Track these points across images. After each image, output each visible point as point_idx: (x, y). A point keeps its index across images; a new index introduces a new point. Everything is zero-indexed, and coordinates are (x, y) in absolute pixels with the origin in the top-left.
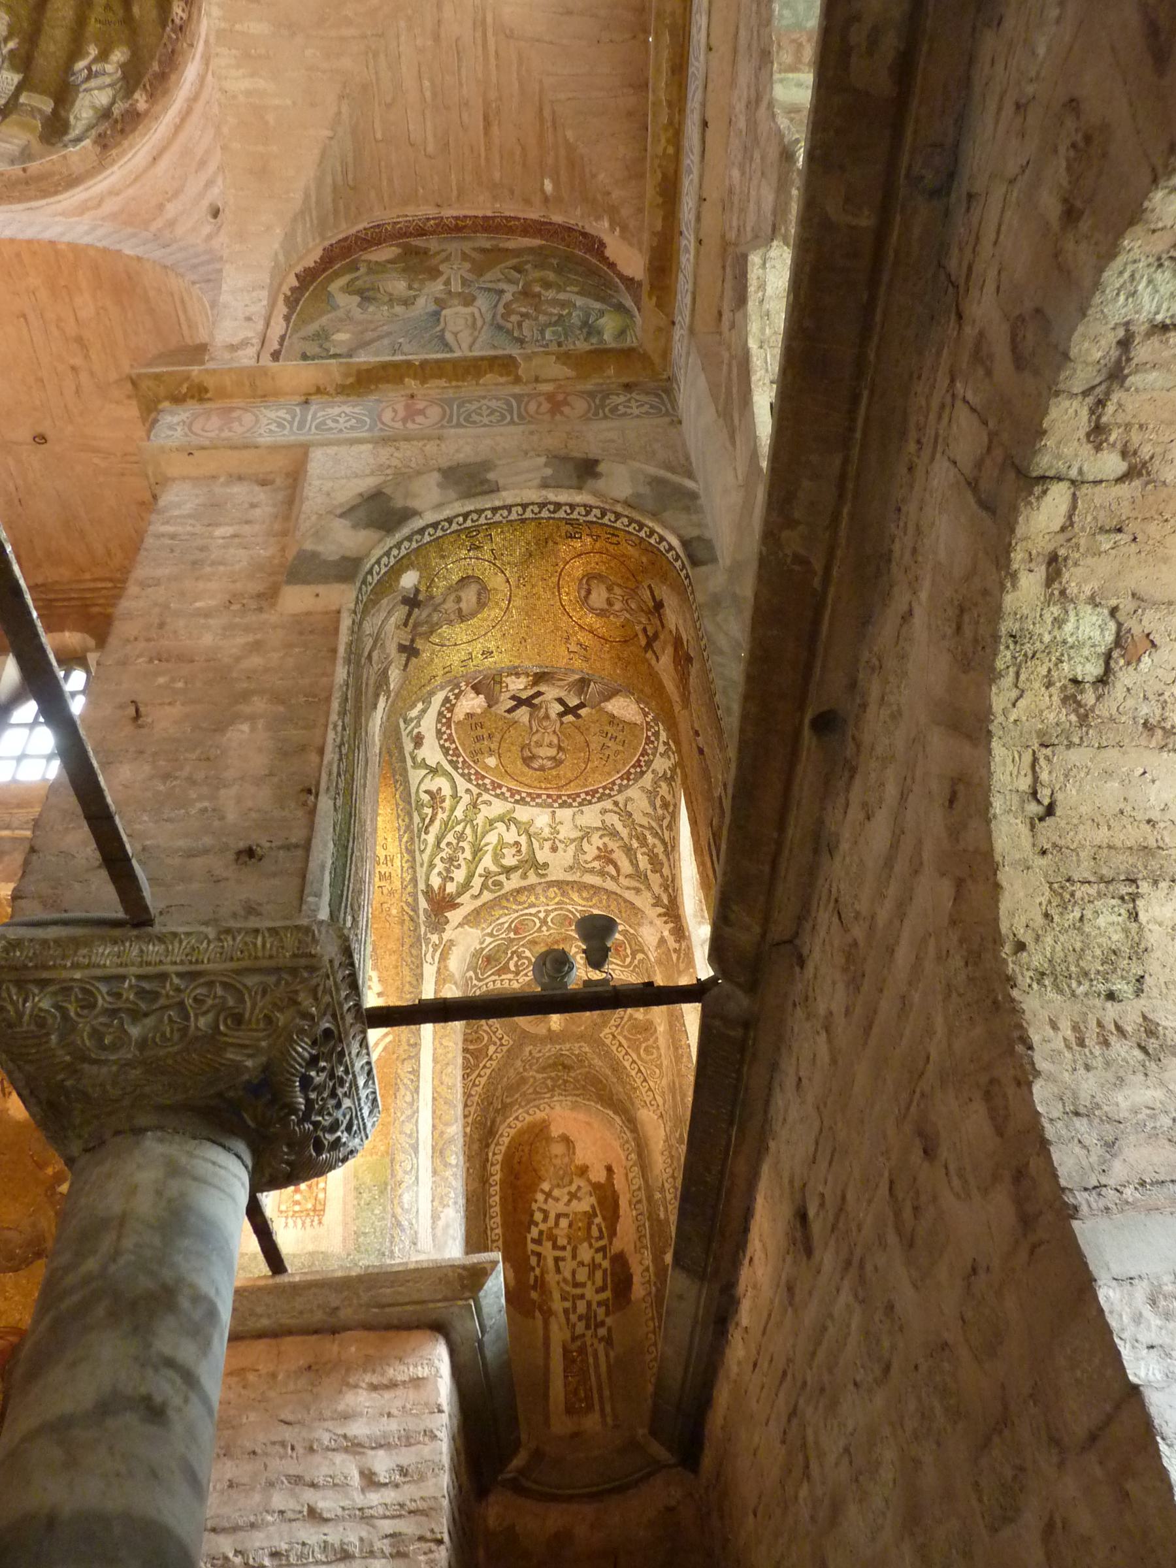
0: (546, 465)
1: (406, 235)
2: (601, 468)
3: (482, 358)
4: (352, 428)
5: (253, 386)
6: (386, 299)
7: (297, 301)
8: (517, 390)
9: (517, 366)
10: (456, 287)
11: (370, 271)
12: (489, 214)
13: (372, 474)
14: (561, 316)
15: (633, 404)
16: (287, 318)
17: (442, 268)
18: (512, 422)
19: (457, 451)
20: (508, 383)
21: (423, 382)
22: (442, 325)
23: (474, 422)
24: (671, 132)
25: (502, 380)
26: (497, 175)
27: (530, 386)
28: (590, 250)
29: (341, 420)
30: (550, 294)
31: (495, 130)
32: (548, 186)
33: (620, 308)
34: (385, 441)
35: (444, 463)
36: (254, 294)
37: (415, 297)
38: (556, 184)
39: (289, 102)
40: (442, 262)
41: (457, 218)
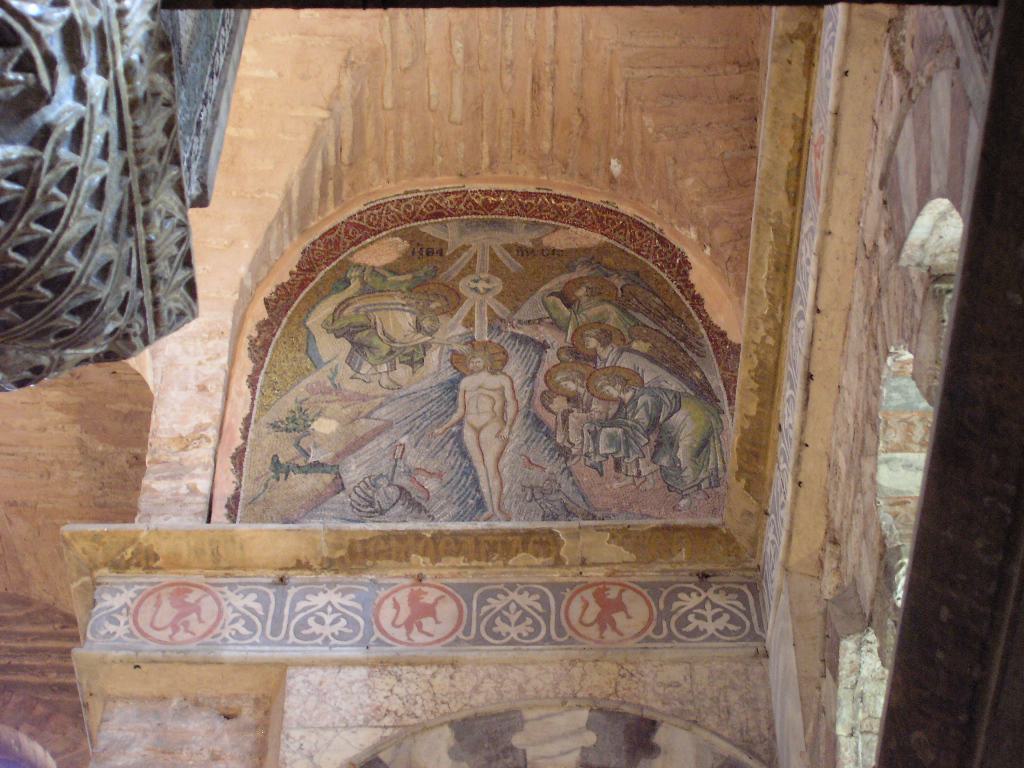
0: (589, 725)
1: (413, 217)
2: (660, 737)
3: (514, 533)
4: (341, 636)
5: (216, 554)
6: (385, 349)
7: (266, 345)
8: (556, 575)
9: (558, 543)
10: (481, 332)
11: (366, 290)
12: (532, 189)
13: (366, 723)
14: (622, 403)
15: (709, 613)
16: (253, 382)
17: (463, 286)
18: (548, 639)
19: (476, 689)
20: (544, 565)
21: (436, 559)
22: (460, 410)
23: (498, 636)
24: (771, 325)
25: (540, 561)
26: (546, 146)
27: (575, 570)
28: (668, 265)
29: (328, 619)
30: (608, 355)
31: (547, 95)
32: (616, 167)
33: (704, 391)
34: (382, 664)
35: (457, 709)
36: (211, 344)
37: (425, 347)
38: (628, 167)
39: (272, 74)
40: (462, 275)
41: (486, 193)
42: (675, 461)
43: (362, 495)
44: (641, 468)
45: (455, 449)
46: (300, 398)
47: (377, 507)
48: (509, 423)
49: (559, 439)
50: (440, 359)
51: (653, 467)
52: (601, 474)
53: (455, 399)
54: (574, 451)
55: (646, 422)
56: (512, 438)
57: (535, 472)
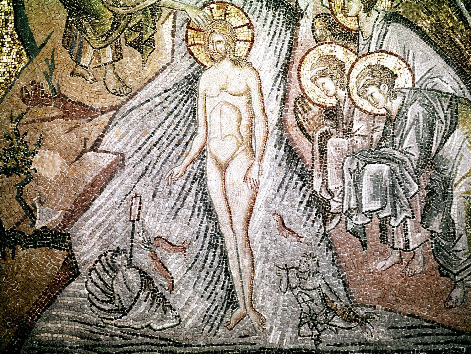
22: (201, 131)
42: (448, 223)
43: (100, 282)
44: (409, 237)
45: (199, 204)
46: (16, 114)
47: (117, 301)
48: (258, 155)
49: (317, 184)
50: (173, 36)
51: (424, 234)
52: (364, 245)
53: (194, 112)
54: (334, 206)
55: (415, 152)
56: (262, 180)
57: (289, 243)
